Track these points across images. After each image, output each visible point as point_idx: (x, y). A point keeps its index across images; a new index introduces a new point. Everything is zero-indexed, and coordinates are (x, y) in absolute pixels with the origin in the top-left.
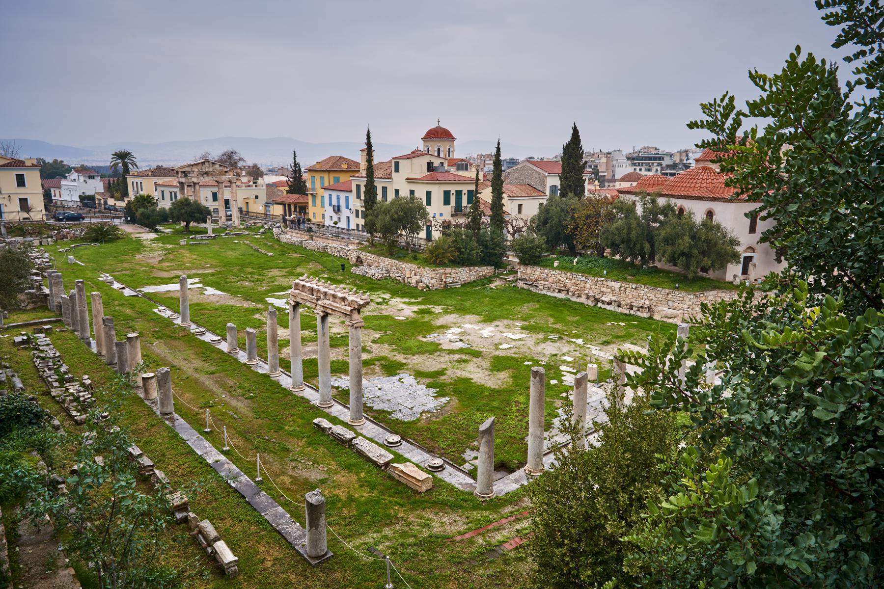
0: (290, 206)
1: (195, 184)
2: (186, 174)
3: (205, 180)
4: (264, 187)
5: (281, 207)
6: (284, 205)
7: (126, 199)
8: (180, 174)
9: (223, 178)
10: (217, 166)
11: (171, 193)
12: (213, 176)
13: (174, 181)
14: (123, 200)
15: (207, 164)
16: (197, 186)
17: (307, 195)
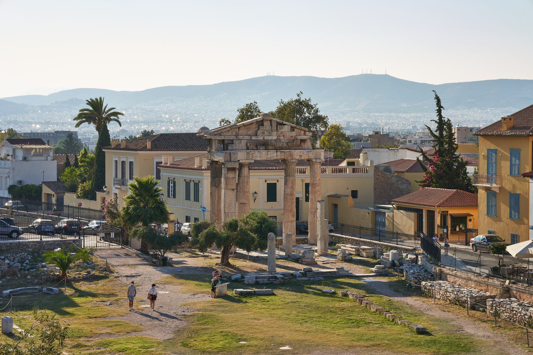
0: (431, 215)
1: (241, 166)
2: (225, 145)
3: (262, 155)
4: (371, 173)
5: (413, 215)
6: (419, 212)
7: (99, 195)
8: (215, 146)
9: (297, 154)
10: (286, 129)
11: (188, 184)
12: (277, 149)
13: (200, 159)
14: (94, 198)
15: (267, 124)
16: (245, 170)
17: (475, 191)
